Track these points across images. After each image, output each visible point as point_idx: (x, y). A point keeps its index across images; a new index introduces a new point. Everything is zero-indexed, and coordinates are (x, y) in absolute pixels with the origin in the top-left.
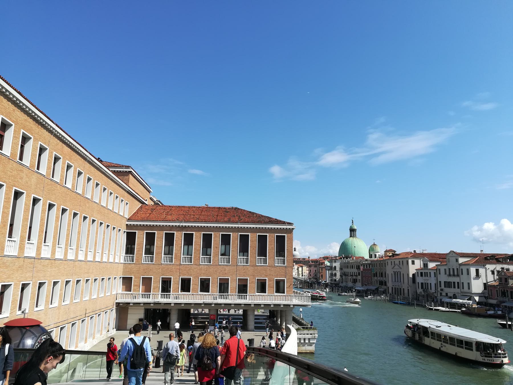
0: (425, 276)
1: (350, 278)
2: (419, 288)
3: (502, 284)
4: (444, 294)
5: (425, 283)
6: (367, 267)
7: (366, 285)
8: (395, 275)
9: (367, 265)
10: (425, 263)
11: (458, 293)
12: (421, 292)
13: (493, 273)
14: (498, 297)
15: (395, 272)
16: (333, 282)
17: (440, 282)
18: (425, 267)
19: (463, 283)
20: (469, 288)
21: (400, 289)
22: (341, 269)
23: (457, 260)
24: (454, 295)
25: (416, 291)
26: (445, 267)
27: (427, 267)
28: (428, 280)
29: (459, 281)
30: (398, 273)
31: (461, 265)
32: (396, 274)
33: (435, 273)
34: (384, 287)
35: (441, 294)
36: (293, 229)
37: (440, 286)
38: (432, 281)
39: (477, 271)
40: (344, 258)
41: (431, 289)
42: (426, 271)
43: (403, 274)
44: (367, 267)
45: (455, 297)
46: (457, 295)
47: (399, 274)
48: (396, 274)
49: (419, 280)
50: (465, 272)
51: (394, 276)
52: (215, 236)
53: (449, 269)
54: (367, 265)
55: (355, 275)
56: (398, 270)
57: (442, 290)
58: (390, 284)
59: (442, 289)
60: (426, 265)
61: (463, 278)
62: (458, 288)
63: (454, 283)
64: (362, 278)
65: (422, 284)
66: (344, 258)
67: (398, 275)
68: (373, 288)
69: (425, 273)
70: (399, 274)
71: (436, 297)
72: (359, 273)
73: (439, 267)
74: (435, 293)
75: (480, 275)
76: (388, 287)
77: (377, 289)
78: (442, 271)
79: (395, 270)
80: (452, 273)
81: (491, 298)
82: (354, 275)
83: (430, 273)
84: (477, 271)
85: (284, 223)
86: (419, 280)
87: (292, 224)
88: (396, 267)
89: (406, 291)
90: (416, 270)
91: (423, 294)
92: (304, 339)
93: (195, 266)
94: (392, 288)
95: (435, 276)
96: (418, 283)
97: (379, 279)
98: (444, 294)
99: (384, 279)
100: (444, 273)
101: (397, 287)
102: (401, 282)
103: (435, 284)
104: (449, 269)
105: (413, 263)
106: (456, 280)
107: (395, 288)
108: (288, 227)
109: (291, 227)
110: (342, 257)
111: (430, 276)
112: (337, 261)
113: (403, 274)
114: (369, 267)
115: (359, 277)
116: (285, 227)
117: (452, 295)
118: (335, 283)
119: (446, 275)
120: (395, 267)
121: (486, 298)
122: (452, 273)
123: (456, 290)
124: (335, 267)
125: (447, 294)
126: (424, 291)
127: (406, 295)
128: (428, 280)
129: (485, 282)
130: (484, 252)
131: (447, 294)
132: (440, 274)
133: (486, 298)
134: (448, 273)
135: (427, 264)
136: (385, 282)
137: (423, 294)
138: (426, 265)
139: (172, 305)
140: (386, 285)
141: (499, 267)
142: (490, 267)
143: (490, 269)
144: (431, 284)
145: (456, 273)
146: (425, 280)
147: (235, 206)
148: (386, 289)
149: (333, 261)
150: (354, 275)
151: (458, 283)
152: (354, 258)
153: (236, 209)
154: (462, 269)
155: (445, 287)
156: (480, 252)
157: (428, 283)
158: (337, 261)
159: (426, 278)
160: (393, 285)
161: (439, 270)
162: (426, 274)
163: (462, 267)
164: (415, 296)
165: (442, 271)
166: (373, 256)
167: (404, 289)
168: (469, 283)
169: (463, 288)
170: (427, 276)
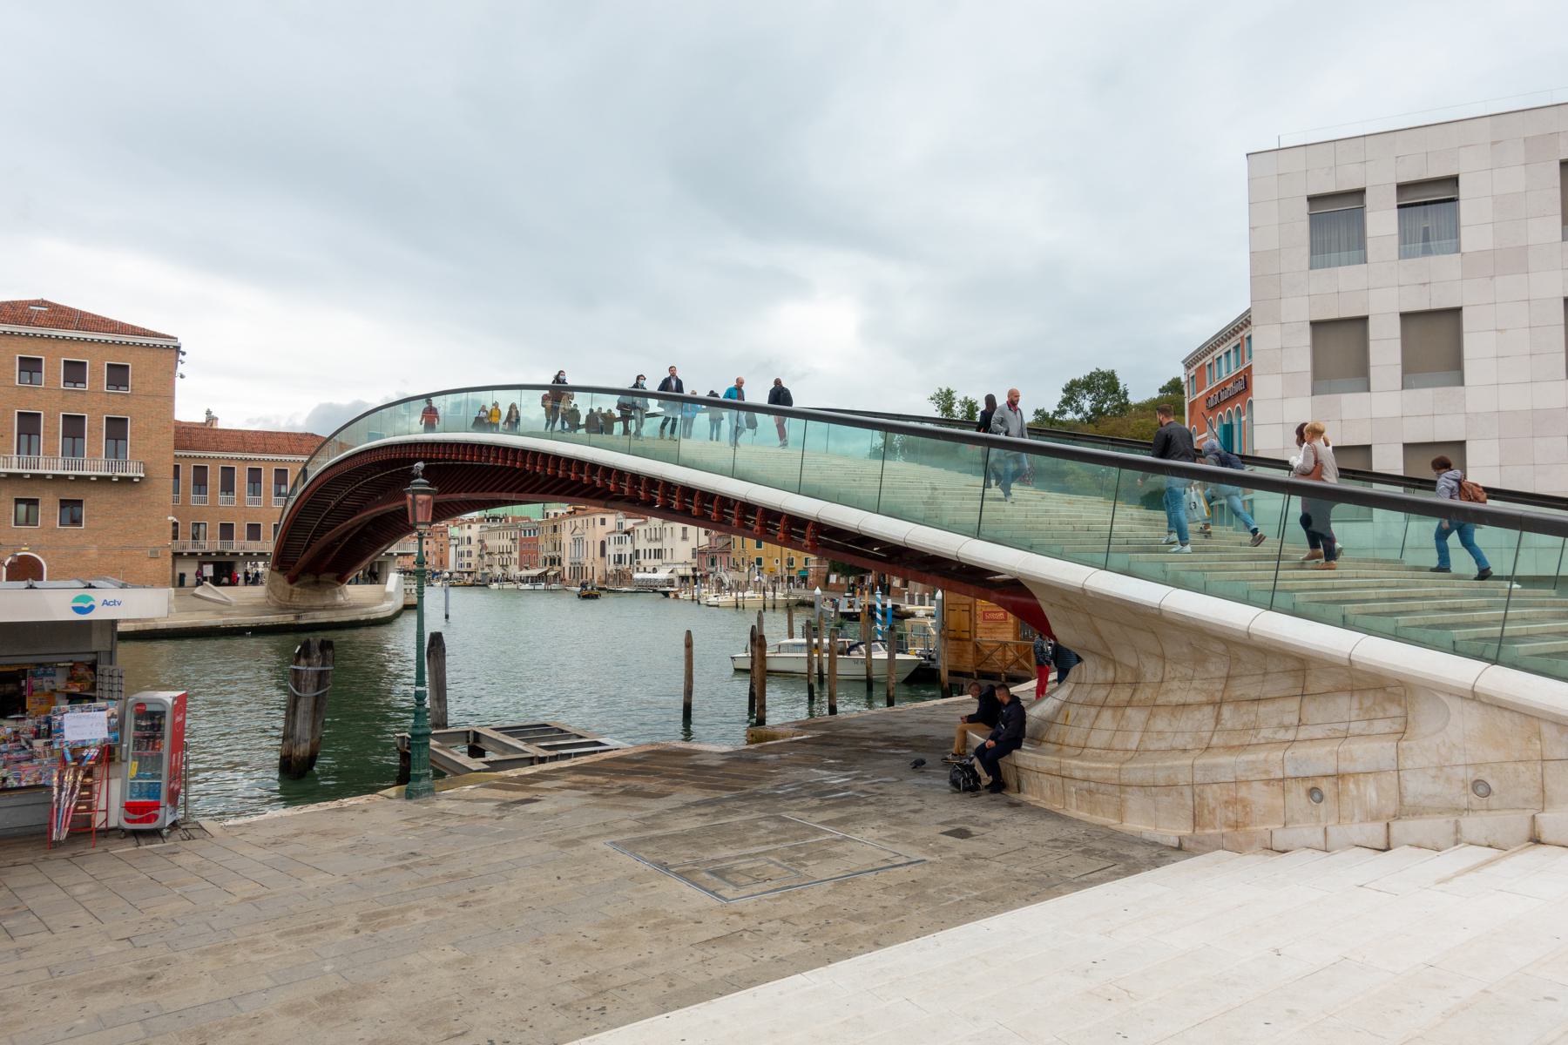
1: (498, 557)
4: (641, 569)
6: (530, 534)
7: (527, 568)
9: (530, 531)
10: (620, 521)
12: (611, 571)
16: (463, 570)
17: (638, 551)
22: (481, 541)
24: (654, 569)
26: (646, 527)
28: (621, 550)
34: (557, 568)
35: (638, 569)
37: (637, 557)
40: (488, 520)
42: (620, 535)
44: (530, 534)
45: (655, 570)
46: (657, 568)
50: (669, 530)
54: (530, 531)
55: (507, 552)
57: (639, 563)
58: (566, 563)
60: (620, 525)
64: (521, 554)
66: (488, 520)
68: (535, 572)
72: (515, 547)
73: (637, 528)
77: (546, 573)
78: (642, 532)
79: (576, 537)
82: (505, 551)
84: (684, 529)
86: (611, 550)
88: (577, 531)
89: (590, 571)
90: (608, 533)
92: (411, 590)
93: (266, 510)
94: (570, 568)
97: (550, 554)
98: (641, 569)
100: (643, 536)
101: (576, 566)
105: (603, 522)
106: (657, 546)
110: (485, 517)
112: (473, 526)
114: (535, 534)
115: (516, 555)
117: (650, 569)
118: (469, 570)
119: (645, 540)
120: (575, 533)
122: (653, 536)
123: (658, 562)
124: (469, 539)
125: (645, 569)
127: (590, 577)
128: (621, 550)
131: (645, 569)
134: (648, 537)
136: (560, 560)
137: (615, 572)
138: (620, 525)
139: (241, 554)
140: (559, 565)
145: (658, 537)
149: (466, 525)
150: (505, 551)
152: (510, 519)
155: (645, 558)
158: (473, 526)
159: (621, 546)
160: (572, 563)
162: (620, 541)
164: (603, 578)
165: (642, 532)
166: (552, 516)
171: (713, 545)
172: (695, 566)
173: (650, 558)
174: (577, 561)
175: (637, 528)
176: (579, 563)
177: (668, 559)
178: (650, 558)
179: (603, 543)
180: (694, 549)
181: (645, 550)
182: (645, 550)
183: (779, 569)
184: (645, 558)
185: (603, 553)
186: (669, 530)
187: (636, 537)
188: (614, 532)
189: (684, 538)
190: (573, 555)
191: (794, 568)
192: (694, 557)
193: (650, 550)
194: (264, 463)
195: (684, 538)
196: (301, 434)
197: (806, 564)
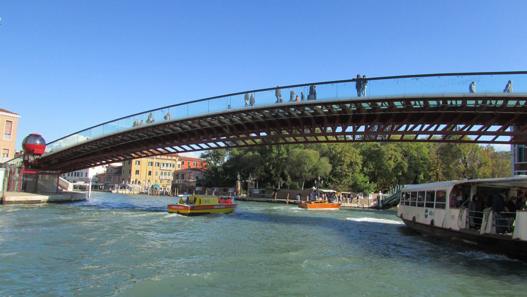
14: (104, 181)
20: (86, 176)
46: (76, 181)
59: (65, 177)
81: (100, 183)
121: (96, 182)
129: (98, 172)
133: (96, 182)
169: (82, 176)
172: (96, 180)
183: (145, 184)
197: (156, 182)
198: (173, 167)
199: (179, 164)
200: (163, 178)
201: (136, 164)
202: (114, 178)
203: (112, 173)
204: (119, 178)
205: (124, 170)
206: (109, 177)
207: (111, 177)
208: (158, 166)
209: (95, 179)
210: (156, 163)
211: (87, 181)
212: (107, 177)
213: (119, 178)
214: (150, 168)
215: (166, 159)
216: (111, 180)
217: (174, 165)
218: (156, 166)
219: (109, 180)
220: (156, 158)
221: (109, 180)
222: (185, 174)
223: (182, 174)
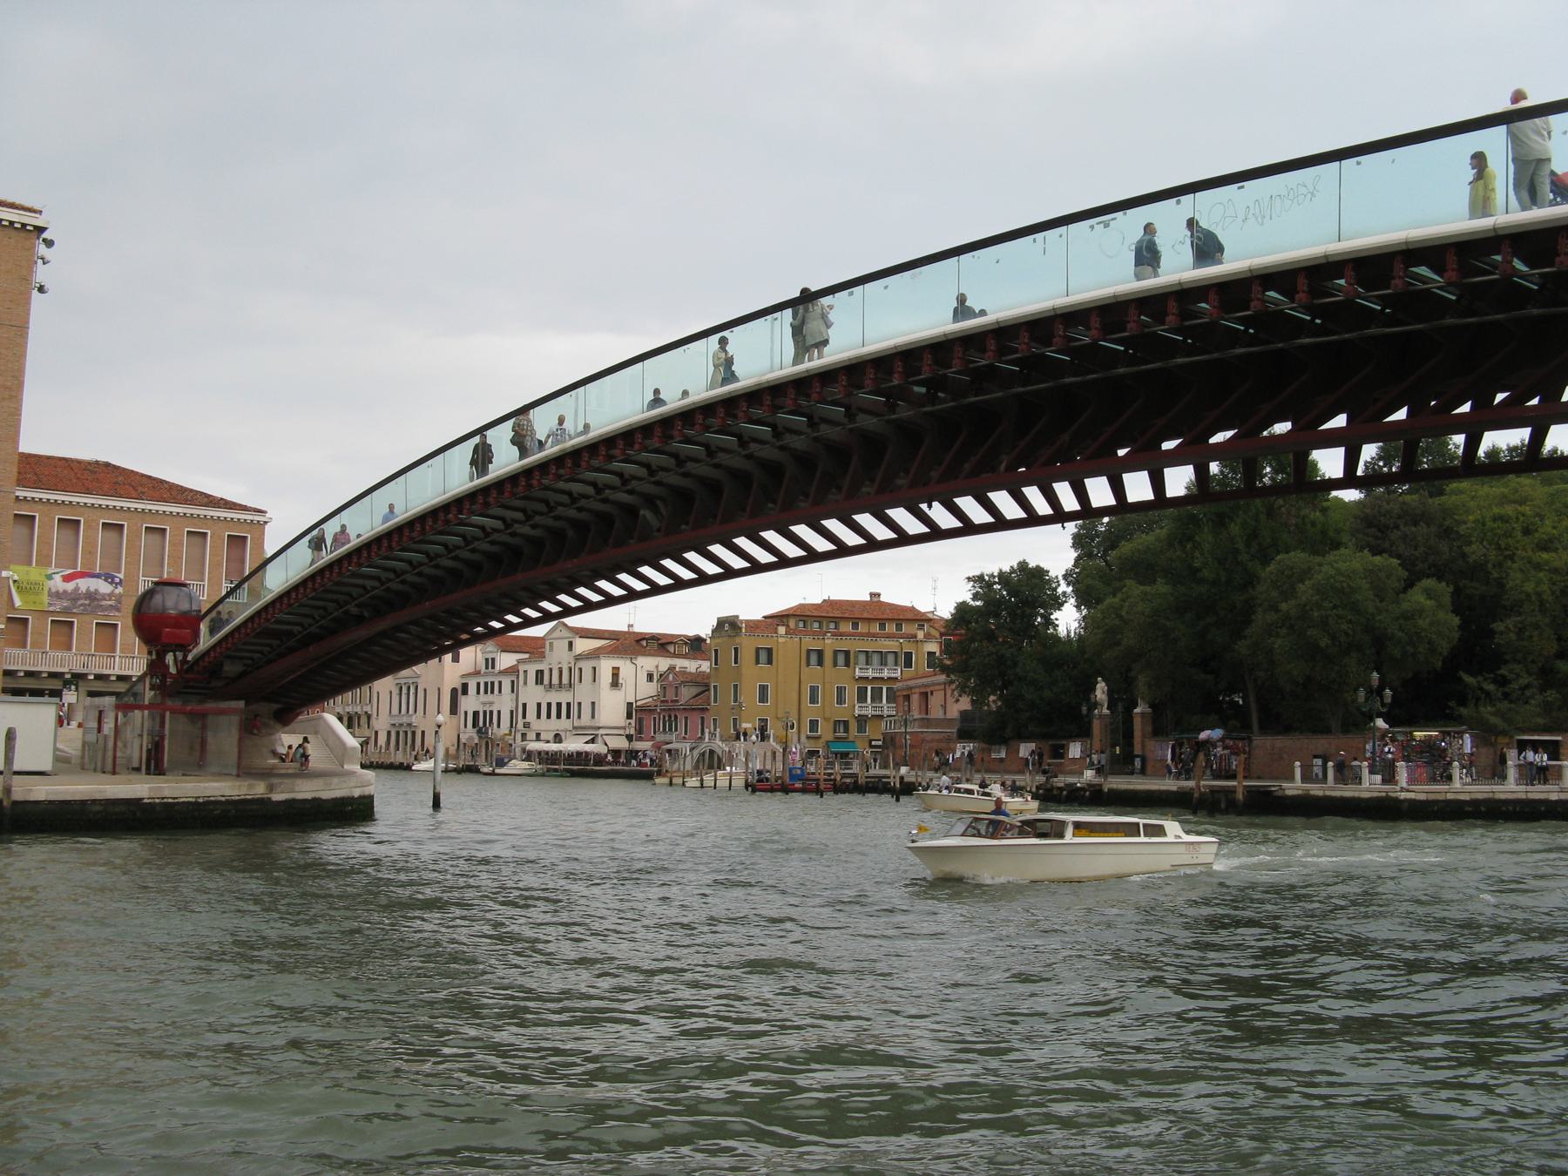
0: (486, 692)
2: (466, 726)
3: (667, 701)
5: (485, 712)
8: (400, 695)
10: (490, 656)
11: (566, 731)
12: (471, 738)
13: (650, 677)
14: (655, 732)
15: (401, 688)
17: (524, 705)
18: (487, 668)
19: (580, 704)
20: (593, 717)
21: (414, 733)
23: (571, 644)
24: (557, 736)
25: (459, 736)
27: (493, 667)
29: (571, 700)
30: (409, 688)
31: (578, 658)
32: (404, 691)
33: (513, 682)
36: (266, 523)
37: (524, 716)
38: (503, 703)
39: (616, 673)
41: (499, 726)
42: (489, 680)
43: (425, 690)
46: (562, 734)
47: (412, 690)
48: (404, 691)
49: (469, 704)
50: (587, 675)
51: (398, 697)
52: (88, 526)
53: (551, 670)
56: (411, 681)
57: (527, 725)
60: (491, 663)
61: (582, 693)
62: (568, 717)
63: (559, 705)
65: (476, 714)
67: (408, 694)
69: (486, 684)
70: (412, 690)
71: (511, 745)
74: (510, 735)
75: (621, 681)
76: (376, 733)
79: (403, 681)
80: (555, 680)
81: (640, 739)
83: (500, 683)
84: (616, 673)
85: (244, 508)
87: (265, 512)
91: (476, 741)
94: (389, 733)
95: (513, 691)
96: (466, 713)
99: (367, 709)
102: (415, 711)
103: (512, 712)
104: (551, 670)
106: (564, 697)
107: (398, 733)
108: (257, 518)
109: (262, 519)
111: (500, 691)
113: (425, 690)
116: (250, 517)
117: (551, 736)
122: (555, 680)
123: (564, 724)
125: (538, 735)
126: (479, 732)
128: (491, 703)
130: (637, 629)
131: (538, 735)
132: (525, 683)
135: (493, 660)
136: (369, 717)
137: (476, 741)
141: (664, 663)
142: (648, 663)
143: (645, 668)
144: (499, 712)
145: (565, 680)
146: (484, 704)
147: (103, 458)
148: (369, 738)
151: (569, 705)
153: (107, 465)
154: (581, 669)
155: (539, 716)
156: (626, 630)
157: (491, 712)
159: (489, 697)
160: (394, 725)
161: (525, 672)
162: (489, 688)
163: (581, 664)
165: (532, 677)
167: (423, 732)
168: (593, 703)
169: (579, 717)
170: (492, 692)
171: (670, 695)
173: (549, 716)
174: (405, 720)
175: (522, 668)
176: (410, 725)
177: (586, 719)
178: (549, 716)
179: (454, 691)
180: (630, 705)
181: (539, 705)
182: (539, 705)
184: (539, 716)
185: (454, 709)
186: (587, 675)
187: (521, 682)
188: (477, 673)
189: (615, 683)
190: (395, 710)
191: (819, 738)
192: (629, 716)
193: (549, 705)
194: (40, 507)
195: (615, 683)
196: (89, 463)
198: (908, 664)
199: (929, 653)
200: (869, 712)
201: (757, 662)
202: (686, 718)
203: (677, 701)
204: (703, 718)
205: (715, 687)
206: (670, 717)
207: (676, 717)
208: (847, 664)
209: (624, 728)
210: (836, 652)
211: (597, 735)
212: (664, 717)
213: (703, 718)
214: (812, 674)
215: (874, 635)
216: (676, 730)
217: (908, 656)
218: (835, 664)
219: (670, 729)
220: (834, 635)
221: (670, 729)
222: (932, 694)
223: (921, 693)
